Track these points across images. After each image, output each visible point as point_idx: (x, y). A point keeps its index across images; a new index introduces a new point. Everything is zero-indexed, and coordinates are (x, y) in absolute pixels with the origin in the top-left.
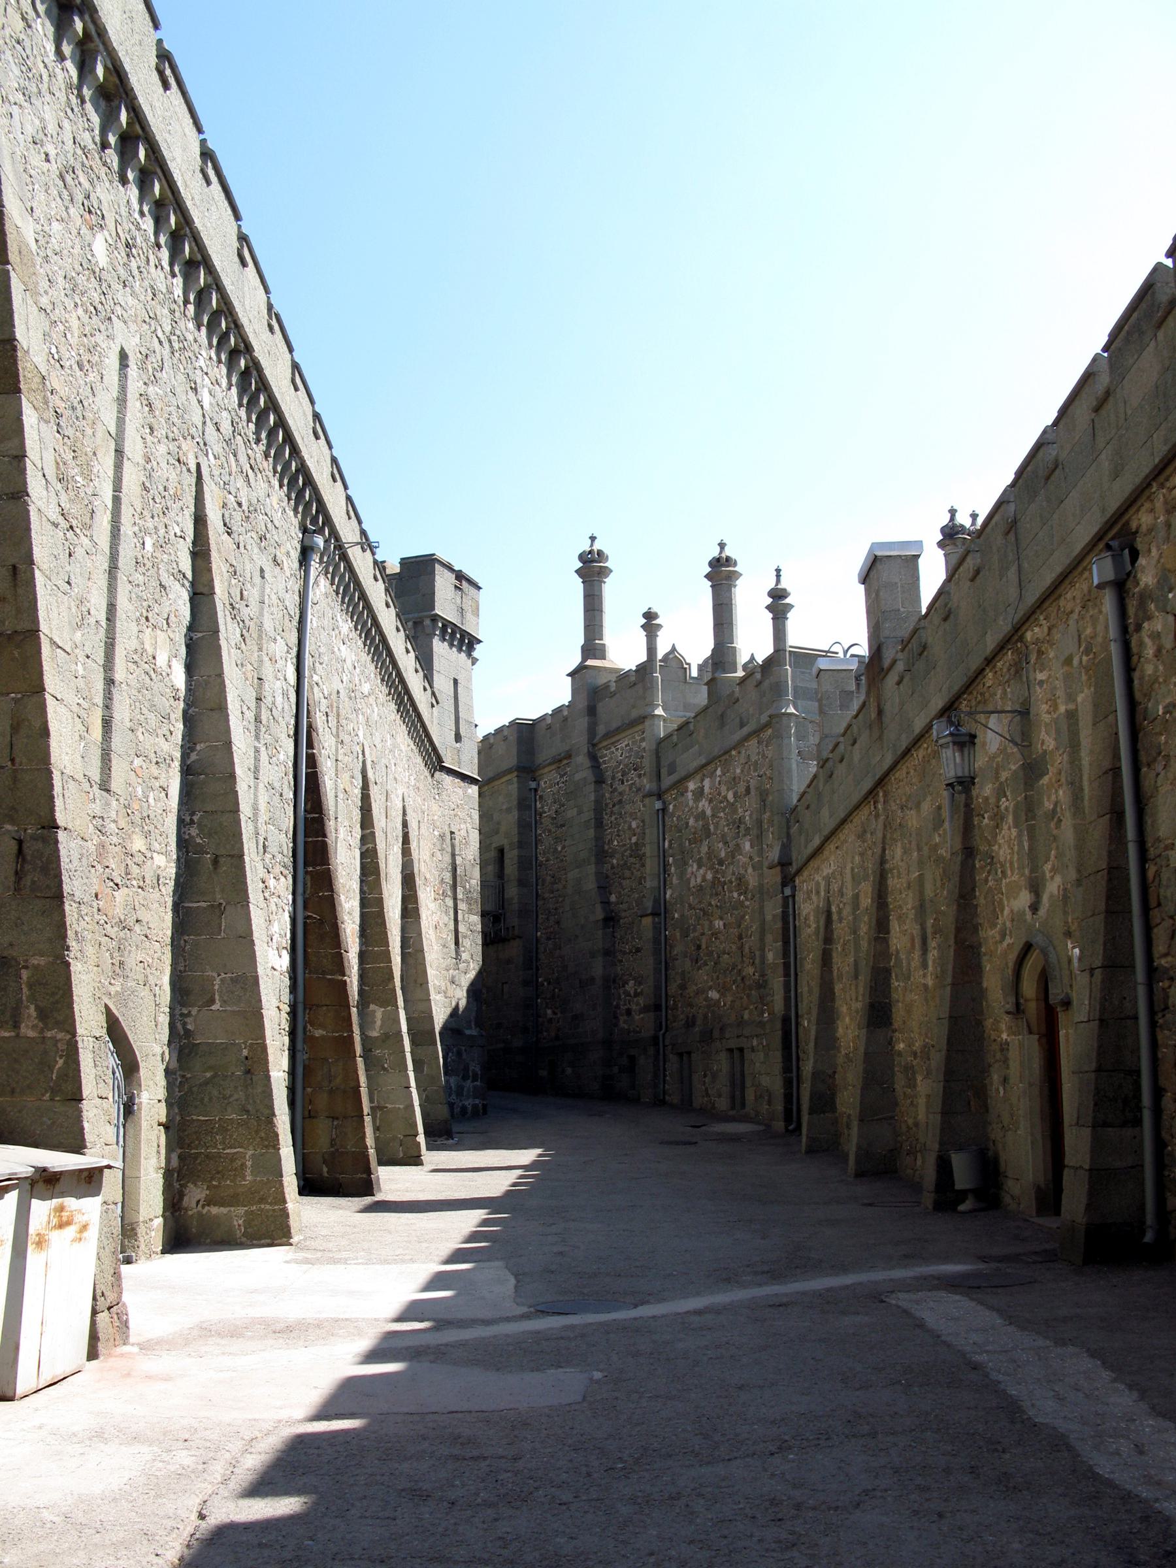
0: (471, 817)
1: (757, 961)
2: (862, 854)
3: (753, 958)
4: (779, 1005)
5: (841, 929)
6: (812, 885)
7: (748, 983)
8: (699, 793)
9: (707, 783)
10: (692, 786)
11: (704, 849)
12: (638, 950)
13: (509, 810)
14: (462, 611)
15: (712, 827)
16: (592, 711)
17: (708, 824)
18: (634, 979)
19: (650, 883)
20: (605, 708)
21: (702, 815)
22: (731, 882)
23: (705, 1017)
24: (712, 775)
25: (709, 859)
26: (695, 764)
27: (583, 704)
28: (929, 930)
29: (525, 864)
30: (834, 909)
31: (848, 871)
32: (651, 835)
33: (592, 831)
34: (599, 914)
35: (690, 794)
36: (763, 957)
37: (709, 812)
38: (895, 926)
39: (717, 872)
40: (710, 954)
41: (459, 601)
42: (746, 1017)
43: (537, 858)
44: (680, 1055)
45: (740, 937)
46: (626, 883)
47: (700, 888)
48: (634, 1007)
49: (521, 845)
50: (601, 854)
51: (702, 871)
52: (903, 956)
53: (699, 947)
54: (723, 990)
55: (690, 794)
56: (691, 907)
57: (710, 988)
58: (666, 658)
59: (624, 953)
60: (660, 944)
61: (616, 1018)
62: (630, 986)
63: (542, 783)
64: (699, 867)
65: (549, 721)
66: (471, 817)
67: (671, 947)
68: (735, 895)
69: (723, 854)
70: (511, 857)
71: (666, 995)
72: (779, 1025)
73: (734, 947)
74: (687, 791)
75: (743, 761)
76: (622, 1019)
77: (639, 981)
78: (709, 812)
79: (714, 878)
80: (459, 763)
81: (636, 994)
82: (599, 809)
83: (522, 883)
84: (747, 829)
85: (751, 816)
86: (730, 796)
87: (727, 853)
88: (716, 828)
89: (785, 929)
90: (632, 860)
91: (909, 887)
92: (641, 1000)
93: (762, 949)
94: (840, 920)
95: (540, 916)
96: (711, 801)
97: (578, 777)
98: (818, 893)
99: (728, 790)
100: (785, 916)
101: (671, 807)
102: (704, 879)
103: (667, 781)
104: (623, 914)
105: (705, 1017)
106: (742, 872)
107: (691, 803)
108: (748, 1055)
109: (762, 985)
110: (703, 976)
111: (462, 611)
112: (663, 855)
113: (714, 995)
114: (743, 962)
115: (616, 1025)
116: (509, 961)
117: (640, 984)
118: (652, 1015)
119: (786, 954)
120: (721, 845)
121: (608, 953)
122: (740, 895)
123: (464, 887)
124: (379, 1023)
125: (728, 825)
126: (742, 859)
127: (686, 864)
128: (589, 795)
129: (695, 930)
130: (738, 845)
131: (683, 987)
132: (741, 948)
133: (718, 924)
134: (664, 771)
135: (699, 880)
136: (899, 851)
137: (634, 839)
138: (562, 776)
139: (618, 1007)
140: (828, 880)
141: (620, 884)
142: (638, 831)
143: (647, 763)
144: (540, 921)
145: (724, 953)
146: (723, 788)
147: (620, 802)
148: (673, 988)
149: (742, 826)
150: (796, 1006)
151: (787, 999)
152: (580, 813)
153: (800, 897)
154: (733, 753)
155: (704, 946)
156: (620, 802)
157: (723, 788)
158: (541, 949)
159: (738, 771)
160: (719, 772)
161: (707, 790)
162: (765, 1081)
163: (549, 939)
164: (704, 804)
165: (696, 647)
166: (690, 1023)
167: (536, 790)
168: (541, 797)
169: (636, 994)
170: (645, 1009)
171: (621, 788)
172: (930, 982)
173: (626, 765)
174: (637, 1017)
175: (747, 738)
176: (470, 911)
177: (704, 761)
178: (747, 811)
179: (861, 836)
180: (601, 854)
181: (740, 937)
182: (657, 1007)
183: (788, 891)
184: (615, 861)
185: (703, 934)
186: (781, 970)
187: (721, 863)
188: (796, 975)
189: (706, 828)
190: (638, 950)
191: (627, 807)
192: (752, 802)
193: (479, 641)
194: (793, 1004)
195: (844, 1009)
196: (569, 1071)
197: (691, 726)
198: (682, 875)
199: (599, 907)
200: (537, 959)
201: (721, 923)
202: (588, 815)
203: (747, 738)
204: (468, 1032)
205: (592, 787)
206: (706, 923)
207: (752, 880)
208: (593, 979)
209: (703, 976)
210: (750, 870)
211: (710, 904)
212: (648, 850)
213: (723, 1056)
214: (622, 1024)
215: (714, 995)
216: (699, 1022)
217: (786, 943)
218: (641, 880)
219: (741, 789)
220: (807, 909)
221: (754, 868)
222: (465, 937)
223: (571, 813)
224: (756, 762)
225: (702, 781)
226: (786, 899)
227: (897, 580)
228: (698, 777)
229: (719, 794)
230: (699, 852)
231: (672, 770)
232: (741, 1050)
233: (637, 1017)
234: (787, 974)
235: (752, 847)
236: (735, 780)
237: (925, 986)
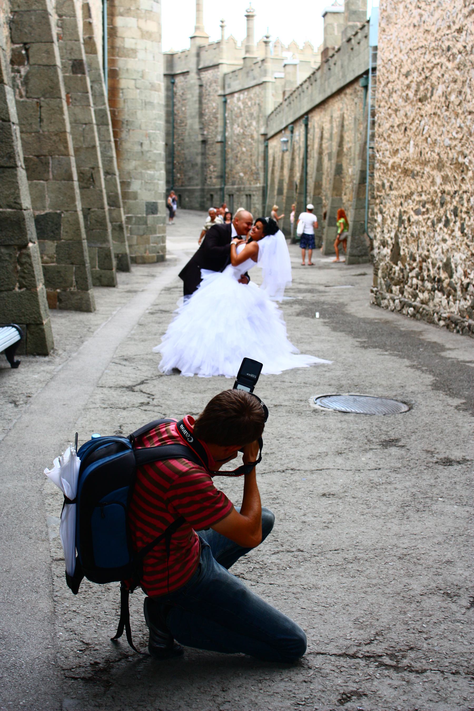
8: (239, 99)
16: (198, 55)
20: (204, 54)
21: (239, 108)
26: (238, 88)
27: (194, 51)
32: (221, 110)
44: (230, 195)
45: (251, 155)
47: (238, 135)
50: (201, 115)
53: (237, 157)
54: (245, 173)
58: (228, 40)
60: (224, 153)
76: (208, 180)
77: (215, 166)
81: (214, 171)
82: (201, 96)
92: (216, 174)
96: (243, 103)
97: (192, 82)
103: (228, 91)
108: (253, 197)
109: (257, 174)
110: (238, 167)
112: (225, 119)
113: (242, 174)
126: (252, 128)
128: (196, 91)
131: (231, 170)
133: (244, 149)
134: (226, 86)
143: (220, 81)
148: (228, 170)
152: (193, 96)
162: (257, 206)
164: (240, 104)
165: (241, 37)
169: (214, 171)
171: (209, 89)
178: (255, 110)
180: (201, 115)
181: (251, 155)
189: (241, 112)
192: (256, 108)
196: (187, 199)
198: (232, 128)
202: (196, 98)
205: (197, 88)
207: (256, 136)
208: (196, 164)
213: (244, 197)
215: (242, 174)
218: (216, 127)
220: (270, 151)
223: (189, 96)
231: (229, 86)
232: (250, 195)
236: (251, 99)
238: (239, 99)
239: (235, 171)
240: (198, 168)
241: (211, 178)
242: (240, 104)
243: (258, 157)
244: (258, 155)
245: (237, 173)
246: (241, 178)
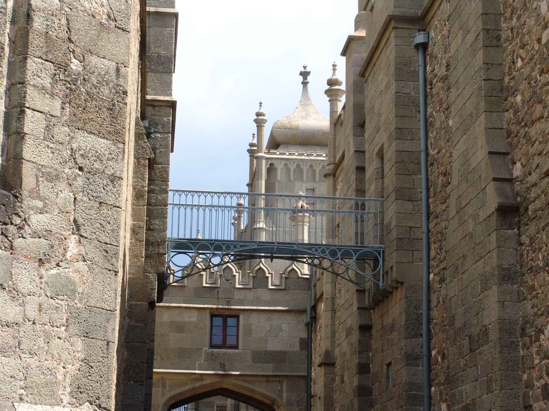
13: (387, 87)
29: (407, 164)
33: (480, 55)
34: (492, 202)
43: (427, 155)
49: (401, 133)
63: (432, 34)
70: (390, 154)
83: (404, 194)
95: (433, 246)
116: (392, 327)
121: (507, 276)
123: (64, 67)
139: (529, 385)
144: (433, 253)
158: (434, 298)
167: (424, 46)
168: (431, 56)
199: (491, 188)
200: (429, 320)
202: (476, 26)
240: (490, 352)
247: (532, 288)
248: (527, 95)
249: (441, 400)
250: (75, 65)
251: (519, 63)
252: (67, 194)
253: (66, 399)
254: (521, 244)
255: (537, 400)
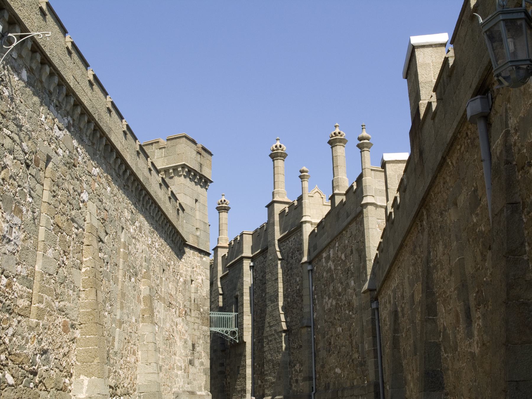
0: (205, 273)
1: (360, 350)
2: (414, 265)
3: (357, 348)
4: (372, 377)
5: (404, 322)
6: (387, 297)
7: (355, 363)
8: (328, 258)
9: (331, 252)
10: (324, 255)
11: (331, 288)
12: (301, 346)
14: (201, 165)
15: (334, 276)
17: (333, 274)
18: (299, 363)
19: (306, 310)
22: (345, 305)
23: (334, 383)
24: (334, 247)
25: (334, 293)
26: (326, 243)
28: (472, 303)
30: (399, 309)
31: (406, 280)
35: (324, 260)
36: (363, 347)
37: (333, 267)
38: (441, 309)
39: (338, 300)
40: (335, 347)
41: (199, 159)
42: (355, 384)
45: (350, 336)
46: (294, 311)
47: (330, 310)
48: (299, 378)
51: (330, 301)
52: (449, 332)
53: (330, 343)
54: (343, 368)
55: (324, 260)
56: (326, 321)
57: (336, 367)
59: (294, 349)
61: (291, 385)
62: (297, 367)
64: (329, 299)
65: (259, 230)
66: (205, 273)
67: (317, 344)
68: (347, 312)
69: (340, 290)
71: (315, 371)
72: (372, 389)
73: (347, 342)
74: (322, 258)
75: (349, 236)
77: (302, 365)
78: (333, 267)
79: (336, 304)
80: (198, 244)
81: (301, 371)
84: (352, 273)
85: (353, 266)
86: (343, 257)
87: (342, 289)
88: (337, 276)
89: (374, 329)
90: (297, 298)
91: (451, 274)
93: (362, 343)
94: (403, 316)
96: (333, 262)
98: (390, 302)
99: (342, 253)
100: (373, 320)
101: (315, 268)
102: (332, 305)
104: (293, 328)
105: (334, 383)
106: (350, 298)
107: (324, 264)
109: (363, 364)
110: (332, 360)
111: (201, 165)
113: (338, 370)
114: (352, 350)
115: (290, 388)
117: (302, 366)
118: (307, 382)
119: (375, 344)
120: (339, 285)
122: (349, 312)
124: (85, 388)
125: (342, 273)
126: (350, 291)
127: (322, 297)
129: (328, 334)
130: (347, 283)
131: (323, 366)
132: (351, 343)
135: (329, 305)
136: (441, 248)
137: (298, 287)
138: (264, 259)
139: (291, 378)
140: (394, 291)
141: (292, 311)
142: (299, 283)
145: (343, 346)
146: (339, 253)
147: (291, 268)
149: (349, 272)
150: (382, 376)
151: (376, 372)
153: (381, 308)
154: (344, 232)
155: (332, 343)
156: (291, 268)
157: (339, 253)
159: (347, 242)
160: (337, 245)
161: (331, 255)
163: (259, 342)
164: (331, 264)
166: (327, 387)
168: (255, 270)
169: (301, 371)
170: (305, 379)
172: (476, 349)
173: (294, 249)
174: (301, 384)
175: (350, 223)
176: (203, 324)
177: (330, 240)
179: (413, 253)
181: (350, 336)
182: (310, 379)
183: (374, 306)
184: (289, 300)
185: (332, 336)
186: (372, 354)
187: (339, 294)
188: (381, 357)
189: (332, 276)
190: (301, 346)
191: (295, 270)
193: (211, 182)
194: (380, 375)
195: (409, 377)
197: (323, 223)
201: (341, 329)
203: (350, 223)
204: (199, 393)
206: (333, 330)
207: (356, 302)
209: (332, 360)
210: (354, 297)
211: (335, 318)
212: (305, 292)
214: (293, 388)
215: (338, 370)
216: (331, 387)
217: (374, 337)
219: (348, 251)
220: (385, 314)
221: (356, 295)
222: (199, 338)
224: (355, 235)
225: (329, 251)
226: (373, 310)
227: (430, 62)
228: (327, 250)
229: (338, 257)
230: (329, 290)
233: (301, 384)
234: (376, 357)
235: (355, 283)
236: (345, 247)
237: (473, 355)
238: (328, 258)
239: (327, 367)
241: (297, 381)
242: (331, 264)
243: (362, 337)
244: (363, 332)
245: (332, 369)
246: (338, 376)
247: (293, 353)
248: (292, 300)
249: (258, 379)
250: (202, 310)
251: (289, 290)
252: (202, 342)
253: (203, 390)
254: (289, 340)
255: (293, 383)
